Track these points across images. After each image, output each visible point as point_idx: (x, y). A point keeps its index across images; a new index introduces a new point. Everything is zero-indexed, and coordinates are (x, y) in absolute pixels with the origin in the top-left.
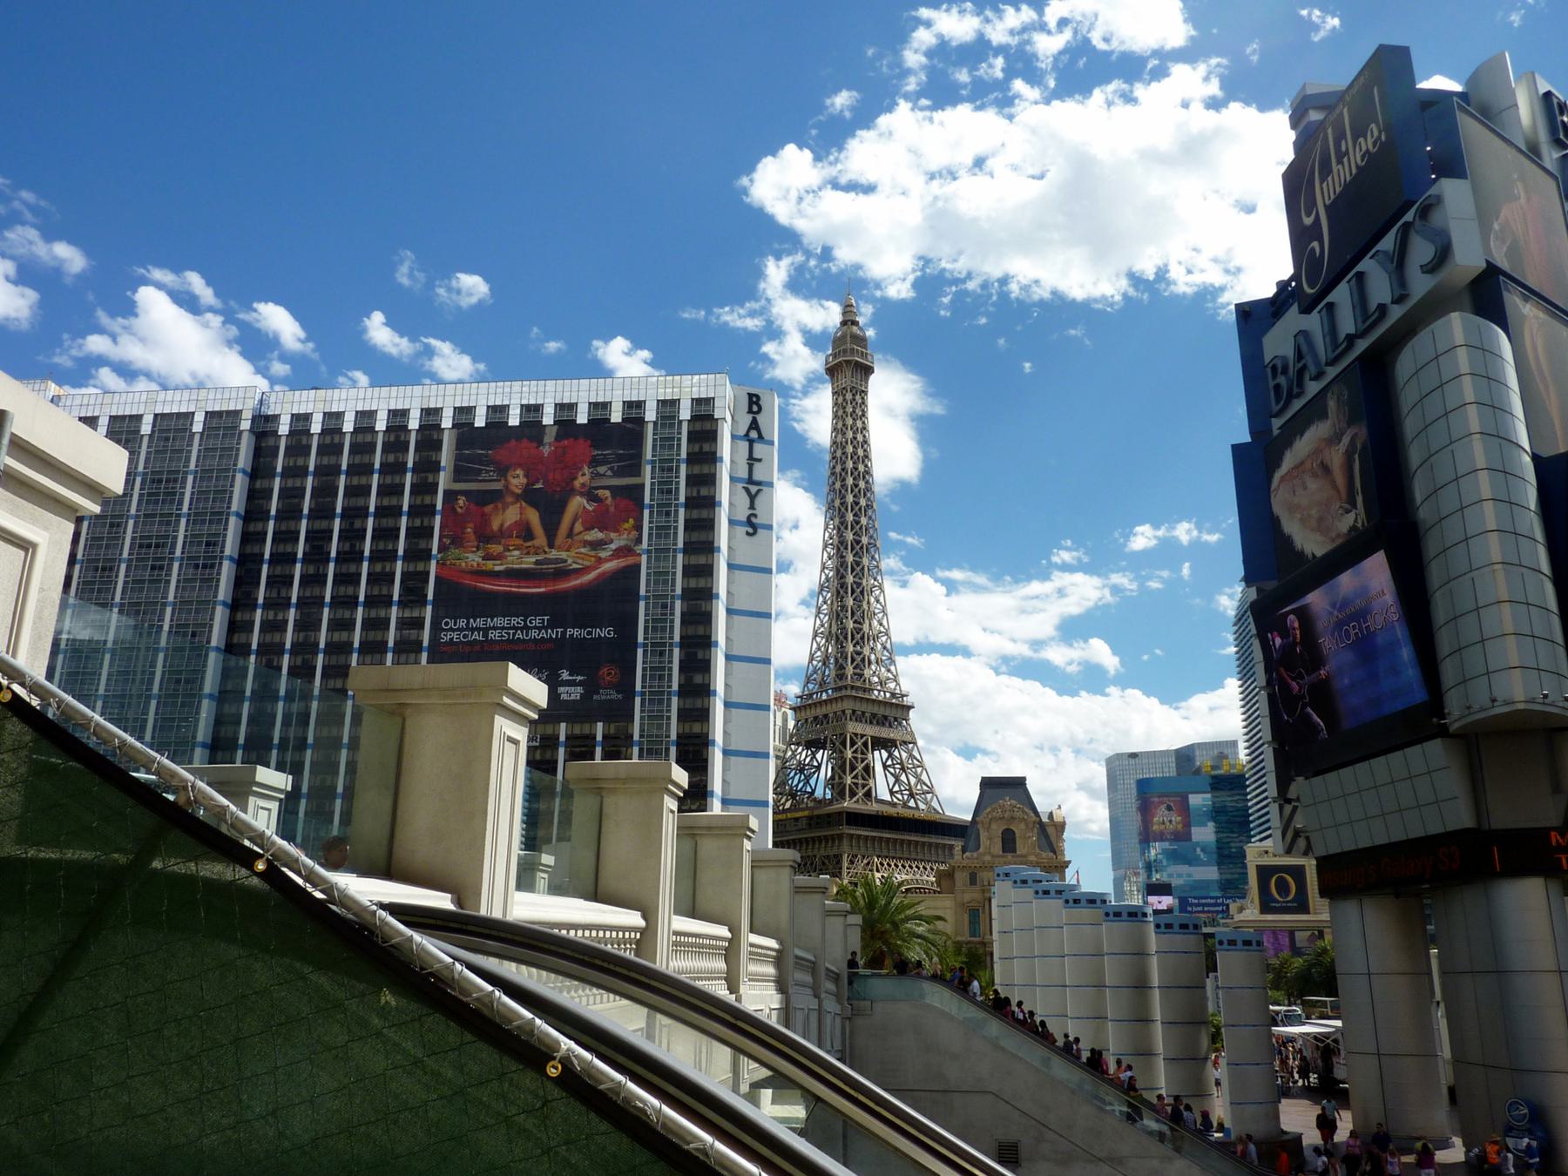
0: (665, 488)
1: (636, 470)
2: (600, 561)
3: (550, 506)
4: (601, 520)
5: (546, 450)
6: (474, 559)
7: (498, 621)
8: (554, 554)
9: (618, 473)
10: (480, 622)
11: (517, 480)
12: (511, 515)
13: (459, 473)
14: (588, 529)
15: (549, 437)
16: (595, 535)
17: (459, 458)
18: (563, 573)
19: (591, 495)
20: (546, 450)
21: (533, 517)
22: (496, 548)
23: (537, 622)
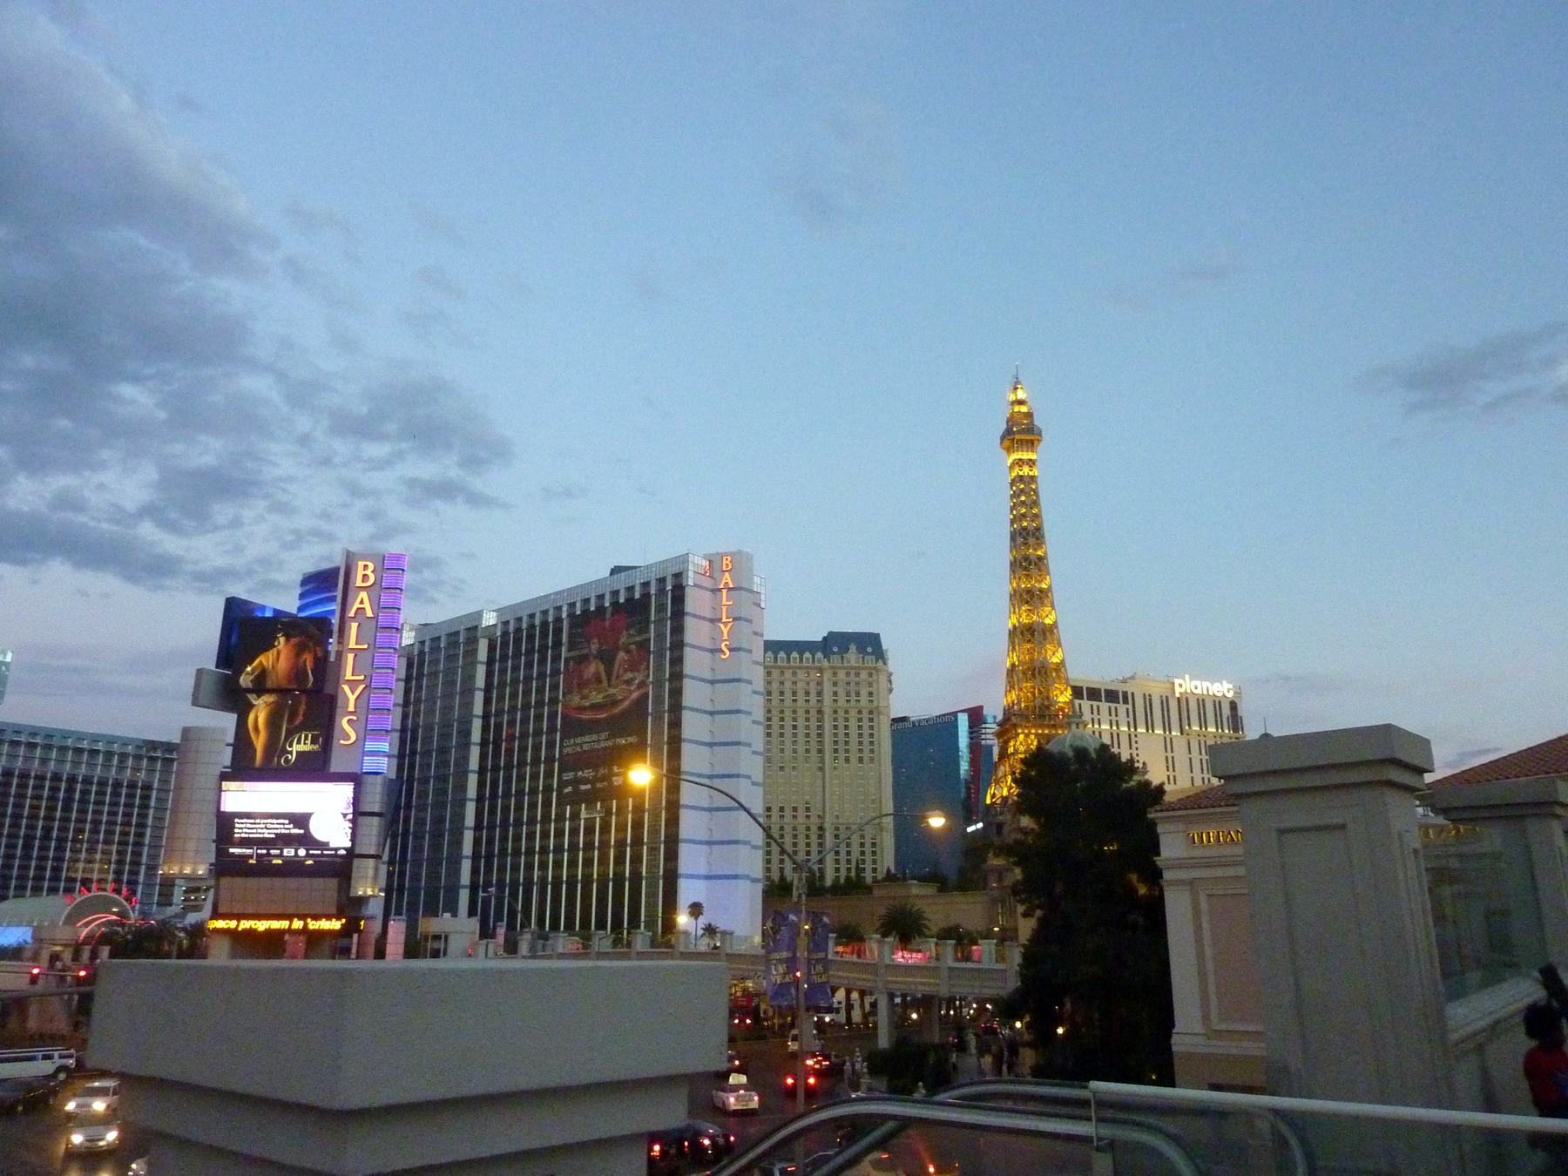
0: (660, 637)
1: (647, 630)
2: (631, 692)
3: (607, 659)
4: (633, 667)
5: (607, 623)
6: (576, 700)
7: (587, 738)
8: (612, 691)
9: (640, 633)
10: (579, 740)
11: (595, 647)
12: (593, 668)
13: (571, 647)
14: (626, 671)
15: (608, 615)
16: (629, 675)
17: (570, 636)
18: (615, 703)
19: (628, 652)
20: (607, 623)
21: (602, 667)
22: (586, 691)
23: (603, 736)
